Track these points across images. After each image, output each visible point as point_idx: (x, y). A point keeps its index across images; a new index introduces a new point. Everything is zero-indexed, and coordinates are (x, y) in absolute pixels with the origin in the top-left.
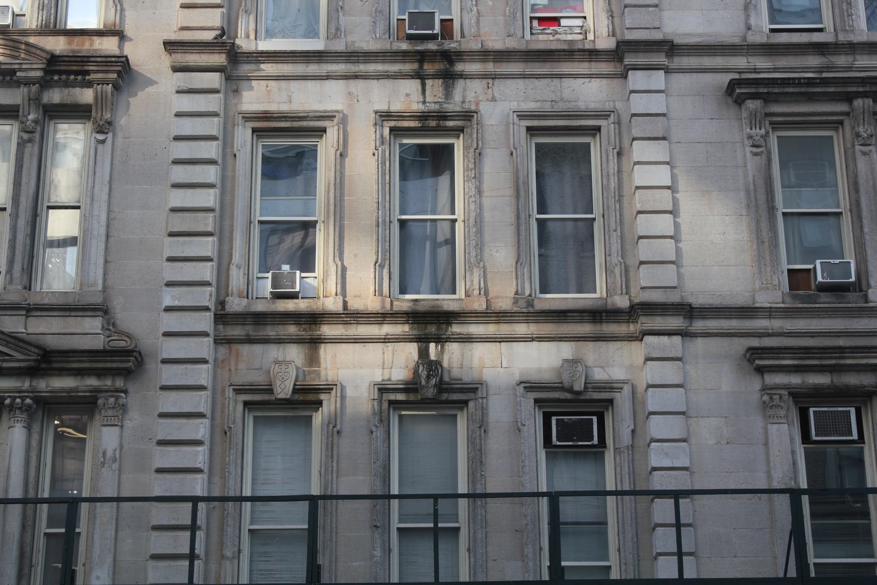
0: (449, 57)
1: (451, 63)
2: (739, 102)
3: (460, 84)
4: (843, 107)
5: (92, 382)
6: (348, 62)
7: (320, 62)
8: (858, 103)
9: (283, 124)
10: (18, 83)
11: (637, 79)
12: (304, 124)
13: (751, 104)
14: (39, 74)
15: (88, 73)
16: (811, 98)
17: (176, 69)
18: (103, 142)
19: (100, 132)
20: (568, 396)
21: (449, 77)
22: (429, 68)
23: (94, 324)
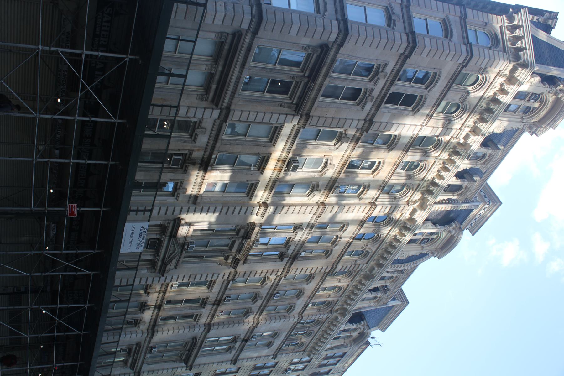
0: (218, 305)
1: (217, 305)
2: (193, 339)
3: (212, 306)
4: (187, 349)
5: (158, 268)
6: (223, 292)
7: (224, 288)
8: (187, 352)
9: (212, 285)
10: (236, 252)
11: (202, 329)
12: (211, 287)
13: (191, 342)
14: (237, 257)
15: (234, 263)
16: (191, 346)
17: (230, 273)
18: (217, 264)
19: (219, 264)
20: (138, 323)
21: (214, 305)
22: (217, 302)
23: (172, 267)
